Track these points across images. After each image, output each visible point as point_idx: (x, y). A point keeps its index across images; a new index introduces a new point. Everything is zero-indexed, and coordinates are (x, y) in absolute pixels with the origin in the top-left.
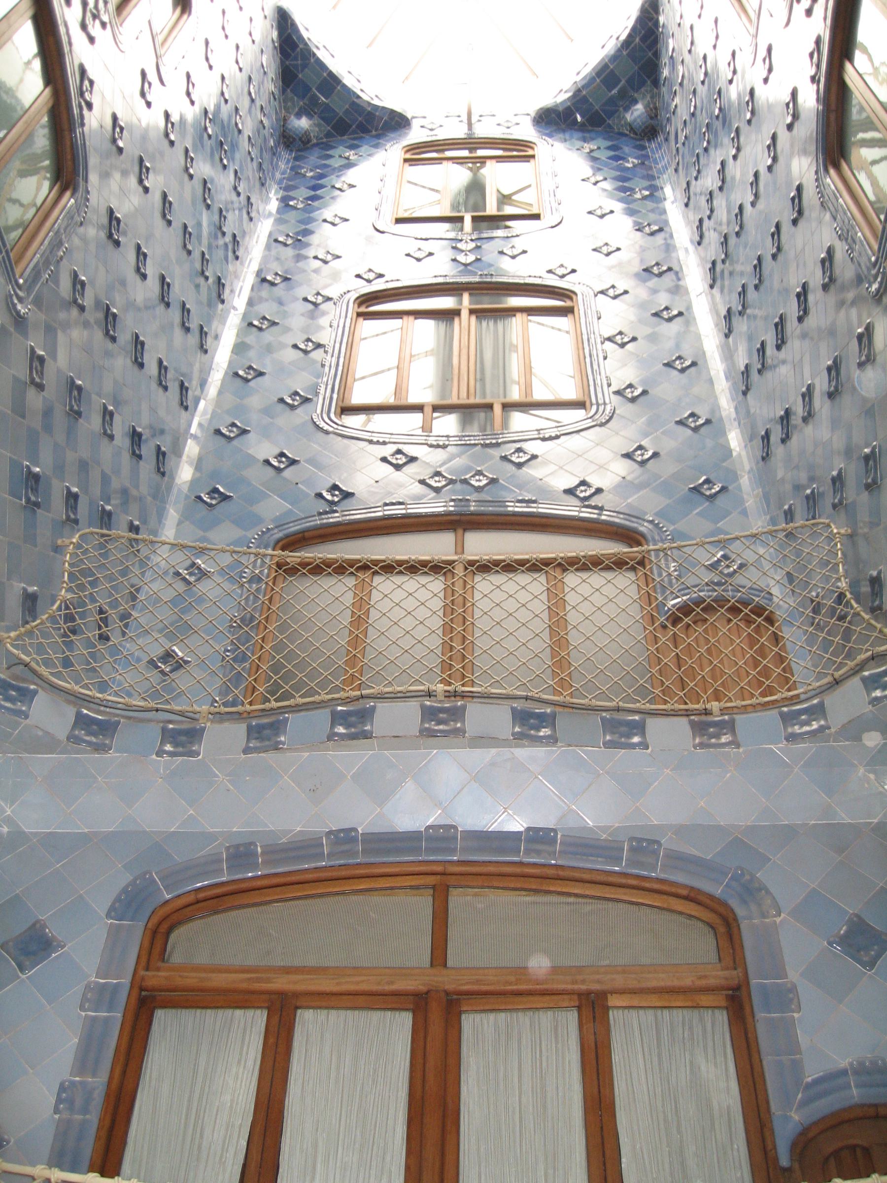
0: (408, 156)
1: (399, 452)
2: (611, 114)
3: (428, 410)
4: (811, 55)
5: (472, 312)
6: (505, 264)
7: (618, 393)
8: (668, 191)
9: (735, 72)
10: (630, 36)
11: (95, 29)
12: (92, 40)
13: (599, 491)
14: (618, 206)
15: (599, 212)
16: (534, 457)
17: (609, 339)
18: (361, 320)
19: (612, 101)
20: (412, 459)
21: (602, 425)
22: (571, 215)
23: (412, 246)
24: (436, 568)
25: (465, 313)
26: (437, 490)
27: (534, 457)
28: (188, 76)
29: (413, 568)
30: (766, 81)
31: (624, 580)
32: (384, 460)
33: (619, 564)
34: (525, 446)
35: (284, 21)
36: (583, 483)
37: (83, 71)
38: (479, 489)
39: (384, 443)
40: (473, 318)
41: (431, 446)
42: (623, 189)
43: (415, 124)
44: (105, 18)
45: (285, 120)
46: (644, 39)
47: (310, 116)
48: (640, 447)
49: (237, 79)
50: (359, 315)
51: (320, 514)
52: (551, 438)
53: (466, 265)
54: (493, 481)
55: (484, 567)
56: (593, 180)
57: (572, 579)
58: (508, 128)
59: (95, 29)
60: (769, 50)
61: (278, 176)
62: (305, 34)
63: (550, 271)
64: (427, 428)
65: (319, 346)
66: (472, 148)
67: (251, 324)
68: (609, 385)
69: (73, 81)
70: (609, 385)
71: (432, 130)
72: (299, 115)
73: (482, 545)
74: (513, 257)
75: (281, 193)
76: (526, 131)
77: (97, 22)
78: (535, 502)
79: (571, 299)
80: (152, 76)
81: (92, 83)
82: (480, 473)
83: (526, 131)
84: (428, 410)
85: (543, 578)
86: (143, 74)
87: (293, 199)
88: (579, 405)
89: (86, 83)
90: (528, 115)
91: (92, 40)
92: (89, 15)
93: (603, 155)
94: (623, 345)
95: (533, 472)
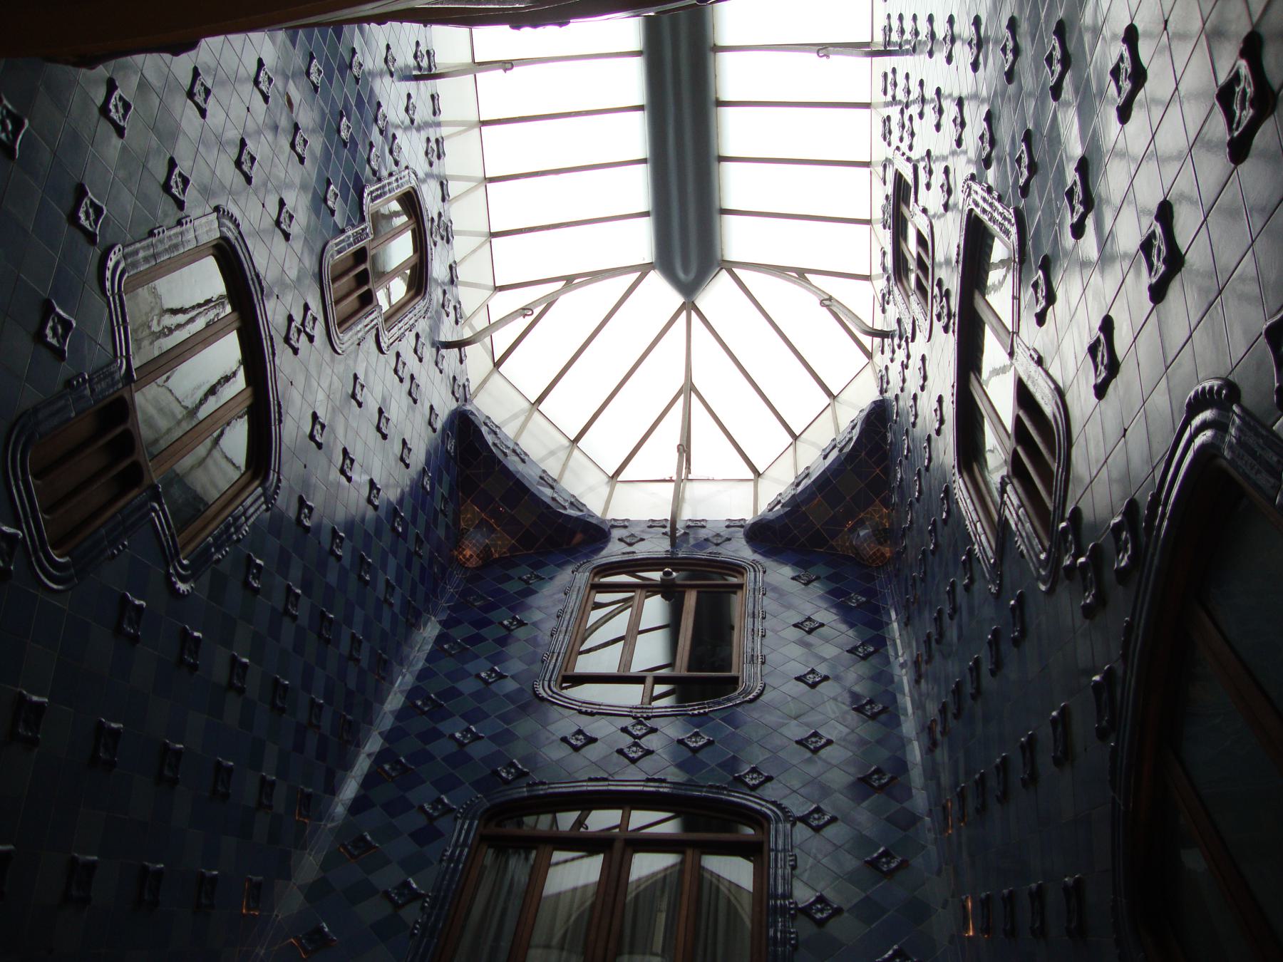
22: (790, 636)
43: (616, 533)
58: (717, 545)
61: (443, 603)
62: (490, 439)
65: (415, 896)
71: (630, 544)
79: (761, 826)
90: (742, 526)
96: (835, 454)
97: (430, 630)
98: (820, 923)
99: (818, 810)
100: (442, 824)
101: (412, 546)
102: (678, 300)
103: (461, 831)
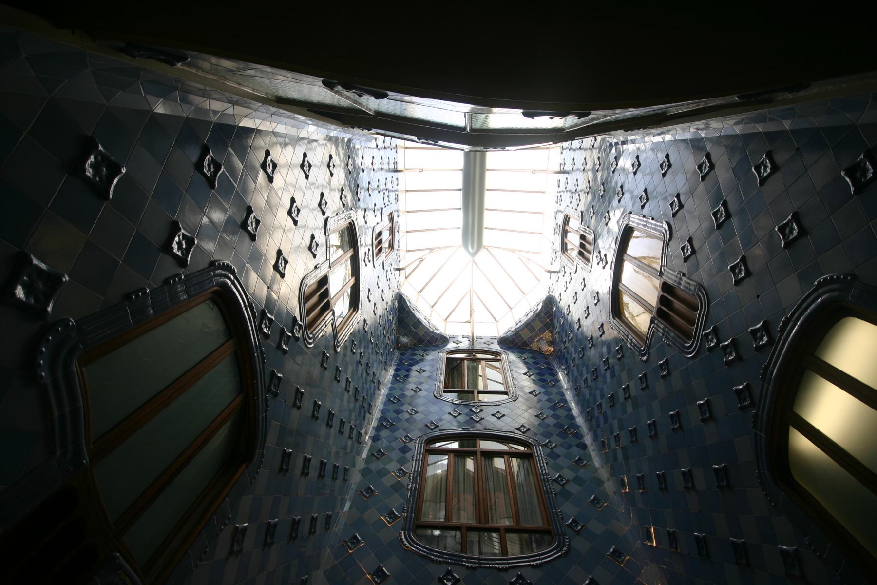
2: (531, 343)
35: (400, 299)
42: (540, 380)
43: (451, 340)
45: (398, 338)
46: (545, 314)
47: (408, 337)
65: (405, 473)
67: (373, 454)
72: (404, 336)
76: (496, 347)
83: (496, 347)
87: (399, 376)
93: (530, 361)
96: (532, 314)
97: (391, 372)
98: (563, 485)
99: (549, 442)
100: (411, 445)
101: (387, 341)
103: (417, 448)
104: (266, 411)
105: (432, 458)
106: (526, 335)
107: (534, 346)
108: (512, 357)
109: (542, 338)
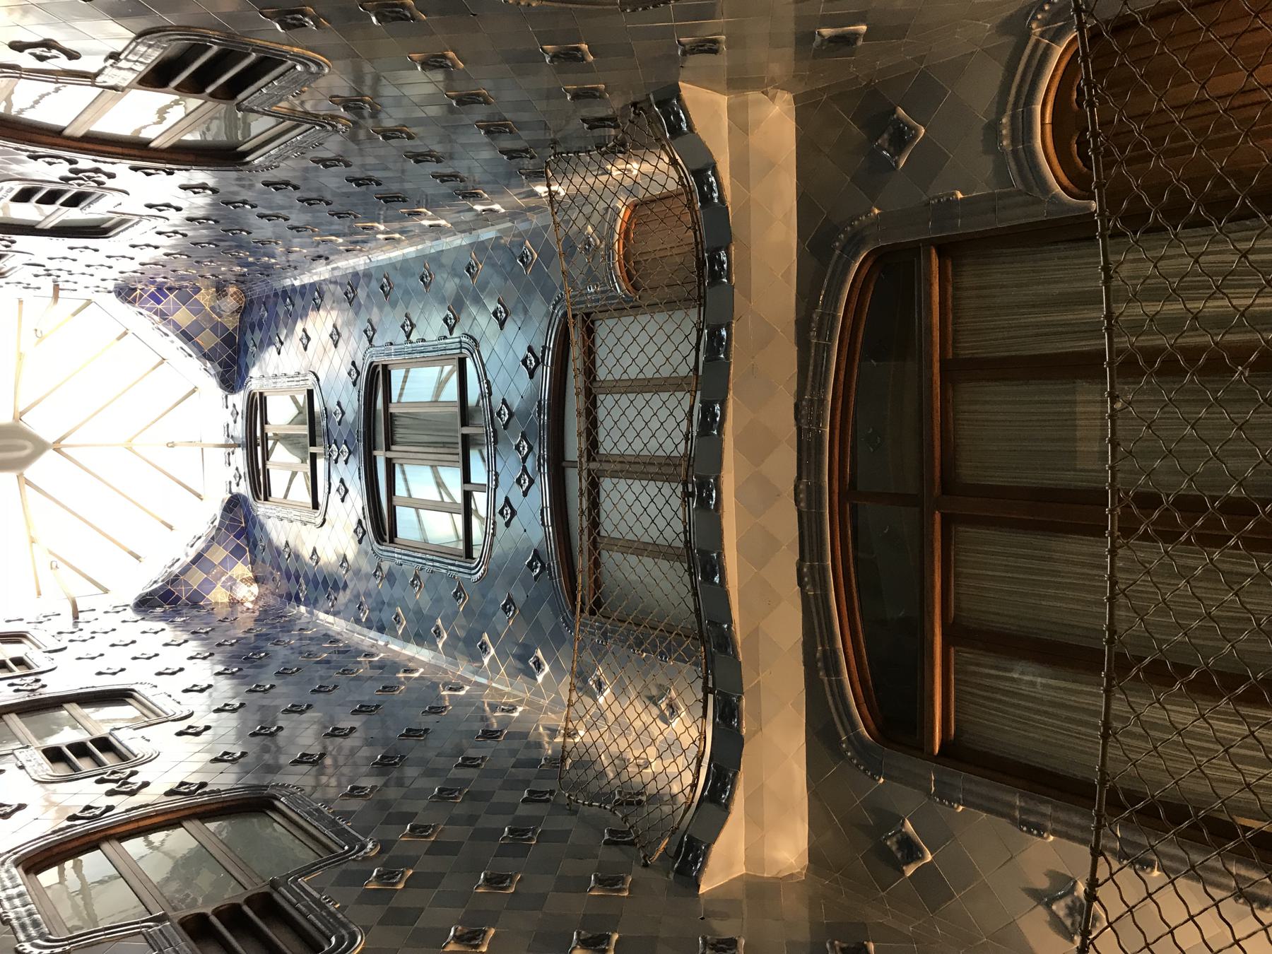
0: (262, 497)
1: (501, 512)
3: (468, 487)
4: (148, 174)
5: (388, 449)
6: (350, 416)
7: (451, 331)
8: (288, 282)
9: (176, 232)
10: (156, 313)
11: (137, 780)
12: (145, 784)
13: (530, 349)
14: (299, 326)
15: (305, 341)
16: (504, 402)
17: (408, 337)
18: (396, 540)
19: (214, 329)
20: (507, 501)
21: (477, 344)
22: (311, 360)
23: (335, 497)
24: (594, 485)
25: (389, 455)
26: (532, 482)
27: (504, 402)
28: (186, 691)
29: (595, 504)
30: (178, 209)
31: (602, 330)
32: (508, 524)
33: (590, 332)
34: (496, 410)
35: (145, 604)
36: (524, 362)
37: (170, 793)
38: (530, 448)
39: (494, 523)
40: (393, 448)
41: (496, 486)
43: (235, 490)
44: (128, 771)
46: (159, 302)
48: (495, 314)
49: (193, 647)
50: (392, 541)
51: (551, 578)
52: (489, 388)
53: (350, 453)
54: (524, 437)
55: (593, 444)
56: (278, 345)
57: (602, 374)
59: (137, 780)
60: (150, 206)
63: (354, 384)
64: (481, 487)
66: (255, 443)
68: (445, 337)
69: (178, 801)
70: (445, 337)
73: (574, 446)
74: (343, 413)
75: (293, 603)
76: (239, 400)
77: (130, 780)
78: (540, 402)
79: (377, 366)
80: (182, 726)
81: (182, 784)
82: (517, 447)
83: (239, 400)
84: (468, 487)
85: (601, 397)
86: (180, 734)
88: (462, 363)
89: (182, 789)
91: (145, 784)
92: (123, 789)
93: (258, 336)
94: (413, 326)
95: (516, 403)
102: (50, 454)
104: (219, 791)
105: (402, 533)
106: (208, 339)
107: (231, 323)
108: (254, 372)
109: (212, 308)
